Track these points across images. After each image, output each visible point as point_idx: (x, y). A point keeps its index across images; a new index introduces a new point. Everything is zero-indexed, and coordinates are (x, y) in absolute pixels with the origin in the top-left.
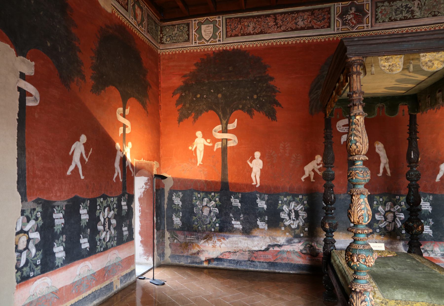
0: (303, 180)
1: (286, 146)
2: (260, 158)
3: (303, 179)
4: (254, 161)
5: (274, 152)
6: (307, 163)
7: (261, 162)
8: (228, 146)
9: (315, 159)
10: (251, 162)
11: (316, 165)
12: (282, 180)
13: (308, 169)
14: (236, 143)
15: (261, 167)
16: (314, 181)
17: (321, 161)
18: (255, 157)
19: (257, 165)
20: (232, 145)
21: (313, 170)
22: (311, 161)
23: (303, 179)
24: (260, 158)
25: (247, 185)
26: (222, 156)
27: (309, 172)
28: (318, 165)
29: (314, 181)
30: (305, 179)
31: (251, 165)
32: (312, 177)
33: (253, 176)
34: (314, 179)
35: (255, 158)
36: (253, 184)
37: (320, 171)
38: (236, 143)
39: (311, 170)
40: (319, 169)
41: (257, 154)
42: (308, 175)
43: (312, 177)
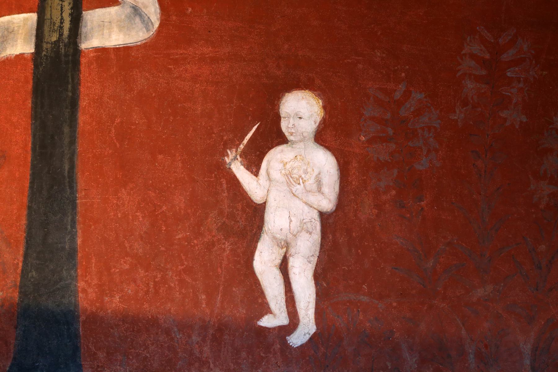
1: (506, 57)
2: (320, 138)
4: (276, 159)
5: (417, 96)
7: (324, 164)
8: (84, 46)
10: (254, 164)
12: (480, 292)
14: (146, 22)
15: (328, 203)
18: (284, 125)
19: (295, 185)
20: (116, 39)
24: (320, 138)
25: (219, 333)
26: (35, 116)
31: (253, 186)
33: (265, 261)
35: (281, 139)
36: (266, 322)
38: (146, 22)
41: (301, 110)
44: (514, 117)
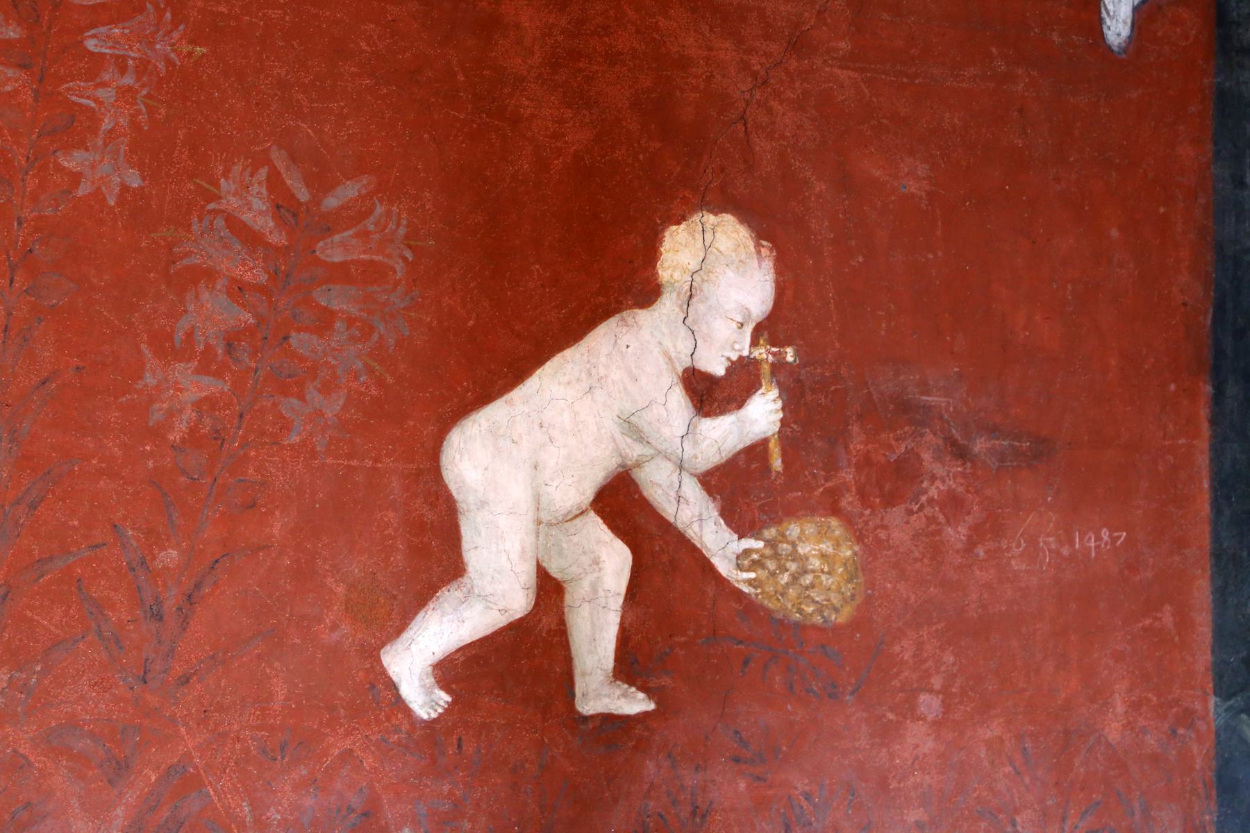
0: (423, 698)
3: (413, 664)
6: (496, 364)
9: (649, 294)
11: (678, 402)
13: (528, 471)
16: (635, 704)
17: (766, 330)
21: (620, 502)
22: (571, 328)
23: (413, 664)
27: (547, 524)
28: (709, 394)
29: (635, 704)
30: (448, 671)
32: (595, 633)
34: (629, 666)
37: (740, 523)
39: (574, 489)
40: (738, 486)
42: (516, 600)
43: (595, 633)
44: (102, 171)
